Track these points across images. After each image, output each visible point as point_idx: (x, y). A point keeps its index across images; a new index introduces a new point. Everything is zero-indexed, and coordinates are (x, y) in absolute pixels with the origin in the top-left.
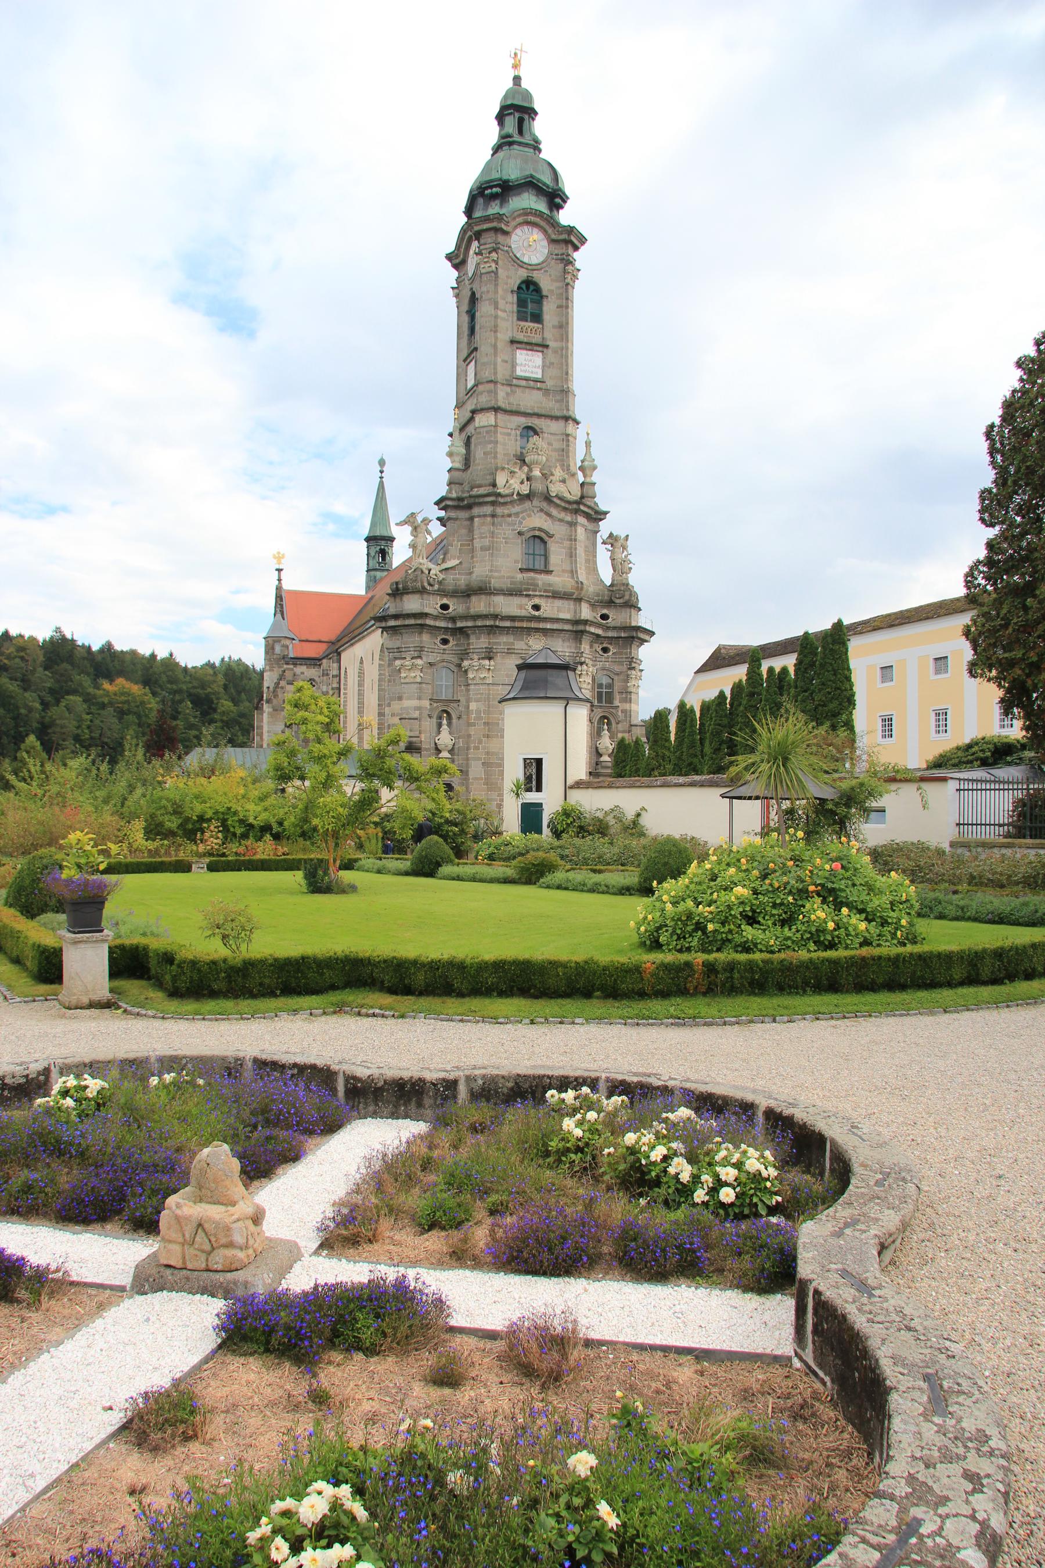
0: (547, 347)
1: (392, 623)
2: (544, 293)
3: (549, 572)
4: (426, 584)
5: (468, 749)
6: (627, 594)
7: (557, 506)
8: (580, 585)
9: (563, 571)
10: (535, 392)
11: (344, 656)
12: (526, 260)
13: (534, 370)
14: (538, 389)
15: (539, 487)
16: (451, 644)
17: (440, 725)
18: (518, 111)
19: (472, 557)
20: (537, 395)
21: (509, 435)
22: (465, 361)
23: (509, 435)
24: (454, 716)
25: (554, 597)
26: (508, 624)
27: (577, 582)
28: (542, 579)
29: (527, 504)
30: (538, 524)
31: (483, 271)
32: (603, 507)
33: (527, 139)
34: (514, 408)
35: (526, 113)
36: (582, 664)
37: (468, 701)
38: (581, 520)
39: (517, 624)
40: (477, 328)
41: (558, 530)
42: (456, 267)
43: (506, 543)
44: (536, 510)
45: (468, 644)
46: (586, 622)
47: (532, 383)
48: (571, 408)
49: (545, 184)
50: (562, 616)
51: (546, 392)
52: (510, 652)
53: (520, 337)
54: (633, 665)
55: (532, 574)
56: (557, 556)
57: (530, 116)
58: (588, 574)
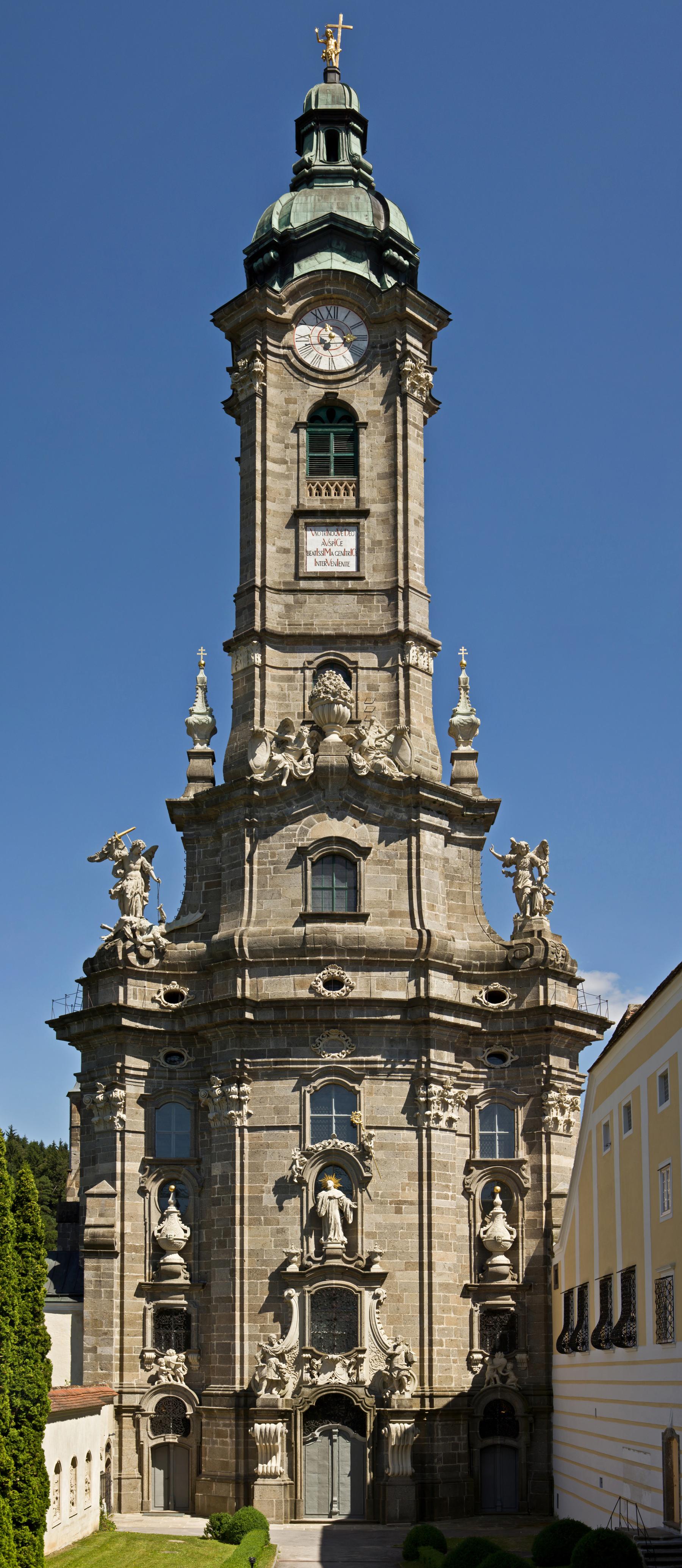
0: (366, 514)
3: (363, 918)
7: (376, 797)
8: (425, 938)
9: (393, 914)
10: (343, 598)
12: (324, 366)
13: (342, 559)
18: (324, 122)
21: (290, 679)
23: (290, 679)
26: (269, 1015)
27: (420, 932)
28: (341, 931)
34: (301, 630)
35: (341, 122)
39: (287, 1015)
43: (276, 870)
47: (335, 584)
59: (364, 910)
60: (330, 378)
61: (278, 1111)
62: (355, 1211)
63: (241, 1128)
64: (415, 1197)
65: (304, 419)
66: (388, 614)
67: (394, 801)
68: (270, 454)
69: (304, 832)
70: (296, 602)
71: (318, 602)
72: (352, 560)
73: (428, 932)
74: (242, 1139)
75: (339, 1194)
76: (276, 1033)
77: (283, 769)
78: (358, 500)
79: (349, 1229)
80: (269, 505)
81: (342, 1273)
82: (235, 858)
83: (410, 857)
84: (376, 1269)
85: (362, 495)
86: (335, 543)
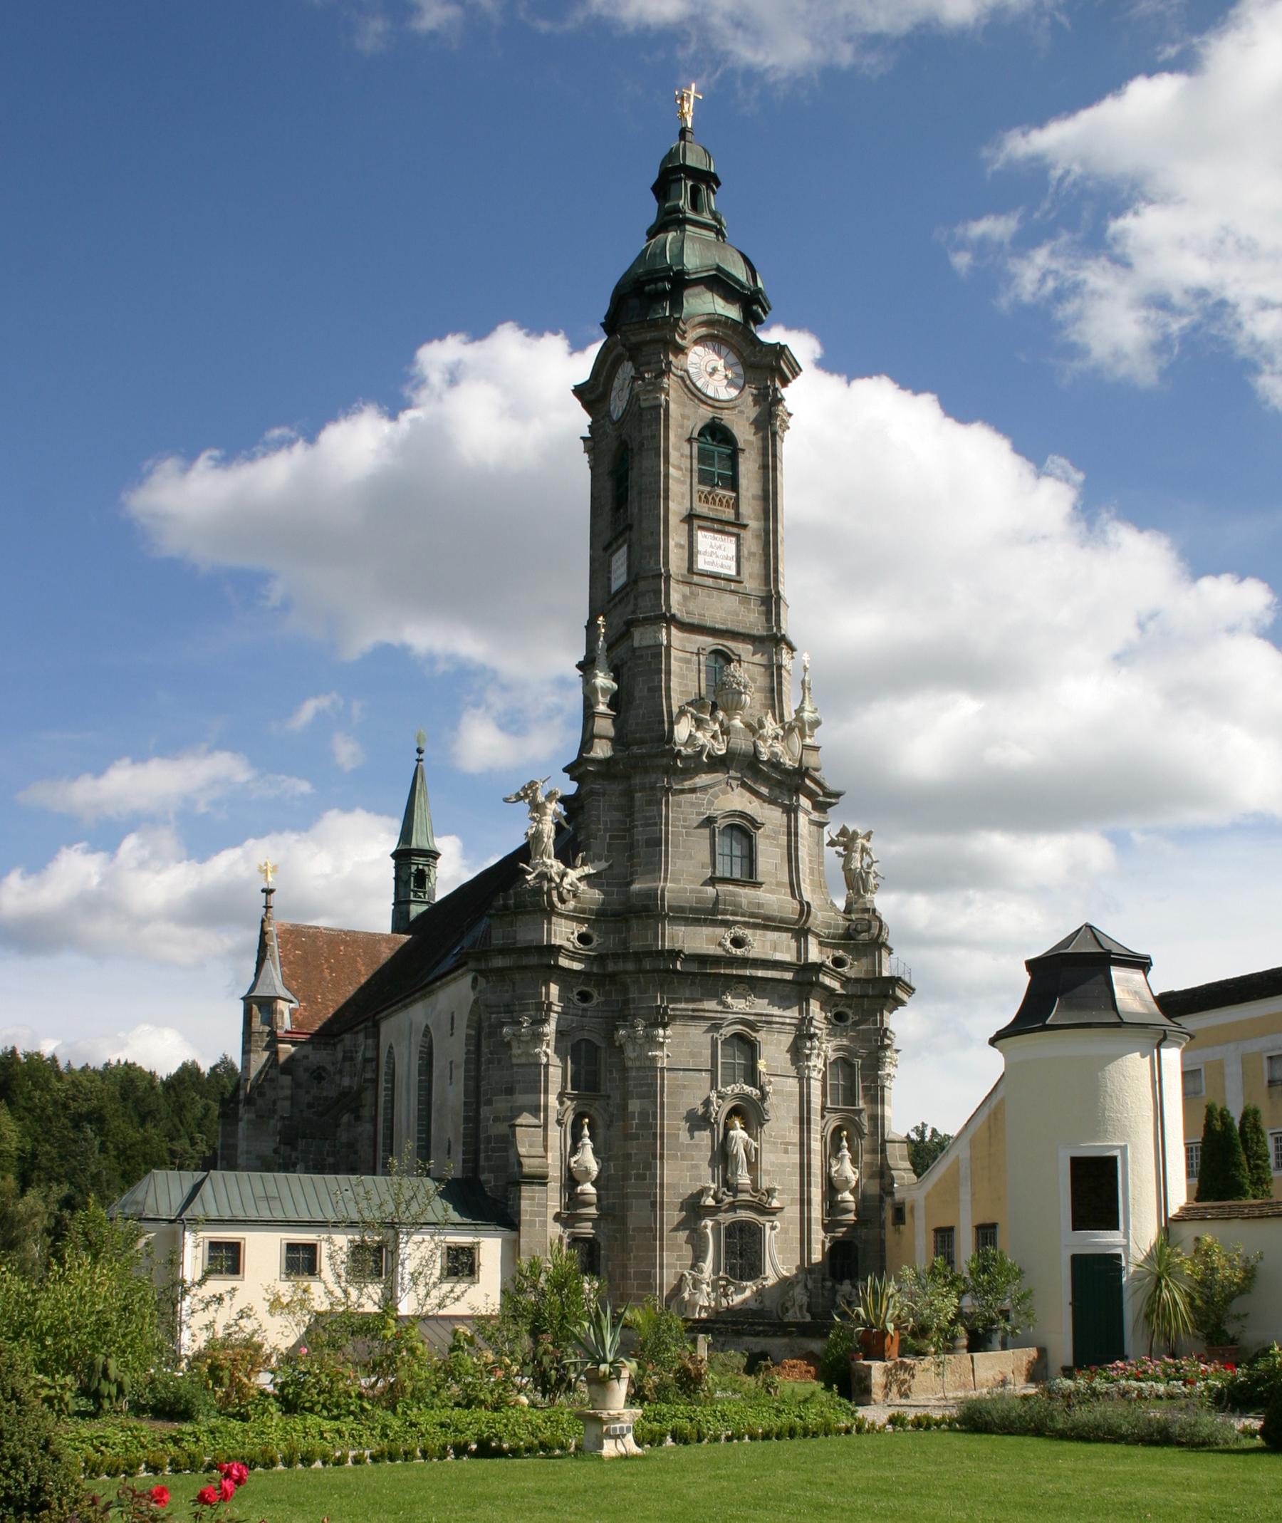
0: (745, 526)
1: (498, 962)
2: (741, 445)
3: (757, 885)
4: (555, 899)
5: (626, 1177)
6: (875, 924)
7: (766, 780)
8: (805, 909)
9: (779, 884)
11: (385, 1027)
12: (710, 393)
14: (732, 592)
15: (742, 743)
16: (595, 1001)
17: (577, 1137)
19: (631, 858)
20: (731, 602)
21: (688, 661)
22: (606, 549)
23: (688, 661)
24: (600, 1122)
25: (766, 927)
26: (694, 968)
27: (801, 903)
28: (746, 895)
29: (719, 776)
30: (738, 807)
31: (644, 405)
32: (831, 785)
33: (706, 217)
34: (695, 620)
36: (811, 1037)
37: (626, 1096)
38: (805, 802)
40: (632, 494)
41: (770, 816)
42: (588, 406)
43: (688, 834)
44: (734, 783)
45: (626, 1002)
46: (818, 968)
48: (783, 624)
49: (737, 281)
50: (779, 956)
51: (745, 597)
52: (695, 1017)
53: (702, 509)
54: (887, 1042)
55: (731, 888)
56: (769, 857)
57: (709, 187)
58: (813, 891)
59: (760, 879)
60: (717, 404)
61: (692, 1055)
62: (756, 1149)
63: (662, 1069)
64: (796, 1140)
65: (695, 435)
66: (763, 618)
67: (779, 784)
68: (672, 460)
69: (711, 803)
70: (691, 593)
71: (709, 596)
72: (733, 564)
73: (808, 904)
74: (662, 1079)
75: (744, 1134)
76: (693, 983)
77: (703, 746)
78: (737, 514)
79: (753, 1167)
80: (671, 505)
81: (748, 1206)
82: (650, 818)
83: (789, 834)
84: (775, 1203)
85: (741, 511)
86: (720, 547)
